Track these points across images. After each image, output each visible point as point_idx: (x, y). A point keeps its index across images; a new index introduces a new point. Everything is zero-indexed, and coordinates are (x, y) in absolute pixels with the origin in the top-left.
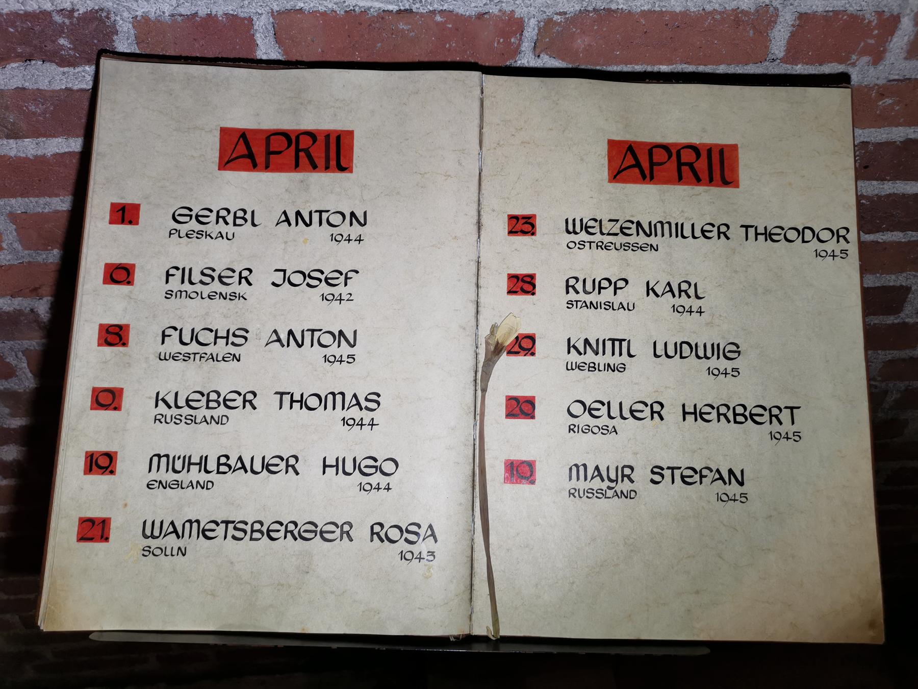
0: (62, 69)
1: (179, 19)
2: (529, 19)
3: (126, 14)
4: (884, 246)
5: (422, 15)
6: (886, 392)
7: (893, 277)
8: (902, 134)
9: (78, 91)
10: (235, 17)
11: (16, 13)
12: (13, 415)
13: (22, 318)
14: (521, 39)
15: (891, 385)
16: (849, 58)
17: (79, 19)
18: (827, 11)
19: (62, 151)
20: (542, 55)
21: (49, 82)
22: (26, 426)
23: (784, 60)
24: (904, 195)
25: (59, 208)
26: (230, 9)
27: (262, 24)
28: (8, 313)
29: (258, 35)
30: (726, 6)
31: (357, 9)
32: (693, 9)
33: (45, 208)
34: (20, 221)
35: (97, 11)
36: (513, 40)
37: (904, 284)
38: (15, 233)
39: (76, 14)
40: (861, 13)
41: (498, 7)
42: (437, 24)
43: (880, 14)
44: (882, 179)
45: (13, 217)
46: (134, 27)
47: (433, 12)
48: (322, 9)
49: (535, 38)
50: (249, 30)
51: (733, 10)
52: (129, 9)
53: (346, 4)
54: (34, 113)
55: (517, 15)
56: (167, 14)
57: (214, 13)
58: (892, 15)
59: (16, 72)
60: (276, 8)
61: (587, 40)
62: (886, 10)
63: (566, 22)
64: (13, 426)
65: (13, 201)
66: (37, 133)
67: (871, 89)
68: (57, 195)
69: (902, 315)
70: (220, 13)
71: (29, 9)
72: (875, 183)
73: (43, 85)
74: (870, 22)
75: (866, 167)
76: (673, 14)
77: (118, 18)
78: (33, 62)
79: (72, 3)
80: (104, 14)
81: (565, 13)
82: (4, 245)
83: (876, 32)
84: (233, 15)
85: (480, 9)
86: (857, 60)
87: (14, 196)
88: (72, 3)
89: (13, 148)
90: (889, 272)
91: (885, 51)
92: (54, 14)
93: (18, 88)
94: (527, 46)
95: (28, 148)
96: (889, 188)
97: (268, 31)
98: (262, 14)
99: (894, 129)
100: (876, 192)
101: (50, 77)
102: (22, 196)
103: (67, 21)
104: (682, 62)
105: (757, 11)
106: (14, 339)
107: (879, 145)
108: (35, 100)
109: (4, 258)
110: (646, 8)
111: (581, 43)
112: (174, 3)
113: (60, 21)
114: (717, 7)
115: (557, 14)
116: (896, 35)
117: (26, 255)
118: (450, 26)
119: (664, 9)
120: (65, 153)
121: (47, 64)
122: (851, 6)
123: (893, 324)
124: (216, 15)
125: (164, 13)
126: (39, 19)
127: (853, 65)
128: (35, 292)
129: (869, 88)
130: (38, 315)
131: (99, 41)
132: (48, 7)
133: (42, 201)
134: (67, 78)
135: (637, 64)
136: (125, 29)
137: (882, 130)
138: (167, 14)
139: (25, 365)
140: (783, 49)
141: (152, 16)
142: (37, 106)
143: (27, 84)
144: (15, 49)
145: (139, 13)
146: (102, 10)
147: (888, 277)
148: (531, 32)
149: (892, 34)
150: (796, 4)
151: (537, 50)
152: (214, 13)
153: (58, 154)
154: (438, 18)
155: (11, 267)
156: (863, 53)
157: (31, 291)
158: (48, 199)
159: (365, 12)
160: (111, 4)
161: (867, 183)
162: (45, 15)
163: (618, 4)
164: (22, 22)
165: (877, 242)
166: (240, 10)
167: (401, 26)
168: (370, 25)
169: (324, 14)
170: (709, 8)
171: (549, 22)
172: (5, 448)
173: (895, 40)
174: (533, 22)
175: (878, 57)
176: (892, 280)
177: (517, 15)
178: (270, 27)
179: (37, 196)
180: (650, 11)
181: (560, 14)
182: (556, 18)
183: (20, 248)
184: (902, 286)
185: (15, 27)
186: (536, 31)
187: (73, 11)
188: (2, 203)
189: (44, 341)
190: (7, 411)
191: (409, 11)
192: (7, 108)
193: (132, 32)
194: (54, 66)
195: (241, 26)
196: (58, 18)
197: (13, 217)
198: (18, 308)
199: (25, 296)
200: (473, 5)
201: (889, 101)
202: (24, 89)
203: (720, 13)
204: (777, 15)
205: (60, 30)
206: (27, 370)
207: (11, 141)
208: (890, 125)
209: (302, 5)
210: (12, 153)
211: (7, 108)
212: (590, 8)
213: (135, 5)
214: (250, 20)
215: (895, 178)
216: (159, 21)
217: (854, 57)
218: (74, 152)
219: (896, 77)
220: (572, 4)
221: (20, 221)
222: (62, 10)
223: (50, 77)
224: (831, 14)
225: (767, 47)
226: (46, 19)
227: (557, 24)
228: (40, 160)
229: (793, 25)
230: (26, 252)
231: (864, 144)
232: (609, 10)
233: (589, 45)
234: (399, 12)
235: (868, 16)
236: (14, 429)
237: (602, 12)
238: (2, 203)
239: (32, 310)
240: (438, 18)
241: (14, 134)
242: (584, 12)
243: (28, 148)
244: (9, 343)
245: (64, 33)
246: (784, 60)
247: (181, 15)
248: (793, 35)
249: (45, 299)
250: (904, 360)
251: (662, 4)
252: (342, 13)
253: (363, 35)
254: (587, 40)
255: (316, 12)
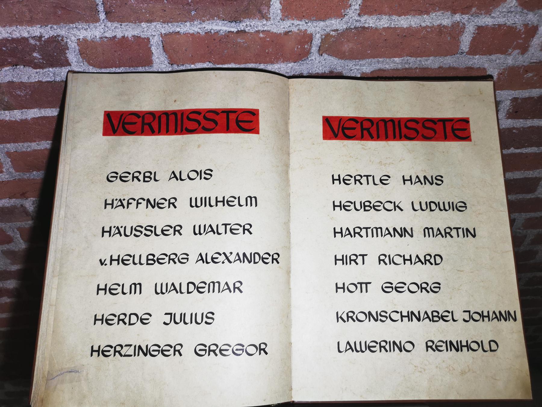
0: (35, 70)
1: (105, 40)
2: (316, 34)
3: (73, 38)
4: (527, 155)
5: (251, 34)
6: (525, 236)
7: (531, 172)
8: (538, 93)
9: (46, 82)
10: (139, 37)
11: (7, 39)
12: (13, 264)
13: (16, 210)
14: (311, 45)
15: (529, 232)
16: (507, 51)
17: (45, 41)
18: (494, 25)
19: (37, 116)
20: (323, 55)
21: (28, 78)
22: (20, 270)
23: (468, 53)
24: (538, 127)
25: (36, 148)
26: (136, 33)
27: (155, 41)
28: (7, 208)
29: (153, 47)
30: (434, 23)
31: (212, 31)
32: (414, 26)
33: (27, 149)
34: (14, 157)
35: (56, 37)
36: (306, 46)
37: (538, 176)
38: (10, 163)
39: (43, 39)
40: (515, 25)
41: (297, 28)
42: (261, 38)
43: (526, 25)
44: (525, 118)
45: (8, 154)
46: (78, 45)
47: (258, 32)
48: (191, 32)
49: (319, 44)
50: (148, 45)
51: (439, 26)
52: (75, 35)
53: (206, 28)
54: (20, 96)
55: (308, 32)
56: (98, 37)
57: (126, 36)
58: (533, 26)
59: (8, 73)
60: (163, 32)
61: (351, 45)
62: (530, 23)
63: (338, 35)
64: (13, 270)
65: (8, 145)
66: (21, 106)
67: (521, 67)
68: (35, 141)
69: (536, 193)
70: (130, 36)
71: (14, 37)
72: (521, 120)
73: (25, 79)
74: (520, 30)
75: (516, 112)
76: (402, 29)
77: (68, 40)
78: (18, 67)
79: (40, 33)
80: (60, 39)
81: (337, 30)
82: (4, 170)
83: (524, 36)
84: (137, 36)
85: (286, 29)
86: (512, 52)
87: (9, 143)
88: (40, 33)
89: (7, 116)
90: (529, 169)
91: (529, 46)
92: (30, 39)
93: (9, 81)
94: (314, 49)
95: (17, 115)
96: (529, 123)
97: (159, 45)
98: (154, 36)
99: (534, 90)
100: (522, 125)
101: (28, 75)
102: (14, 142)
103: (38, 43)
104: (407, 56)
105: (452, 26)
106: (11, 222)
107: (525, 100)
108: (20, 88)
109: (4, 177)
110: (386, 26)
111: (346, 47)
112: (102, 31)
113: (34, 43)
114: (428, 24)
115: (333, 31)
116: (535, 37)
117: (17, 175)
118: (268, 39)
119: (397, 26)
120: (39, 117)
121: (27, 68)
122: (509, 21)
123: (531, 198)
124: (127, 37)
125: (96, 36)
126: (21, 42)
127: (510, 54)
128: (24, 195)
129: (519, 67)
130: (26, 208)
131: (57, 54)
132: (26, 35)
133: (26, 145)
134: (39, 75)
135: (381, 58)
136: (73, 46)
137: (526, 91)
138: (98, 37)
139: (19, 236)
140: (468, 47)
141: (89, 38)
142: (21, 92)
143: (15, 79)
144: (7, 60)
145: (81, 37)
146: (59, 36)
147: (528, 172)
148: (317, 41)
149: (533, 36)
150: (476, 21)
151: (321, 51)
152: (126, 36)
153: (34, 118)
154: (261, 35)
155: (8, 182)
156: (514, 49)
157: (21, 195)
158: (29, 144)
159: (217, 33)
160: (64, 32)
161: (517, 120)
162: (25, 39)
163: (369, 24)
164: (10, 44)
165: (522, 153)
166: (142, 34)
167: (239, 40)
168: (220, 40)
169: (193, 35)
170: (423, 25)
171: (328, 35)
172: (9, 282)
173: (535, 40)
174: (318, 36)
175: (524, 49)
176: (530, 174)
177: (308, 32)
178: (160, 43)
179: (23, 142)
180: (388, 28)
181: (334, 31)
182: (332, 33)
183: (13, 171)
184: (536, 178)
185: (7, 47)
186: (320, 41)
187: (41, 37)
188: (2, 147)
189: (30, 222)
190: (9, 261)
191: (243, 32)
192: (3, 93)
193: (77, 48)
194: (31, 69)
195: (142, 44)
196: (32, 42)
197: (8, 154)
198: (13, 204)
199: (16, 198)
200: (282, 27)
201: (530, 75)
202: (13, 82)
203: (430, 27)
204: (465, 28)
205: (34, 48)
206: (20, 239)
207: (6, 112)
208: (530, 88)
209: (179, 30)
210: (7, 119)
211: (3, 93)
212: (352, 27)
213: (78, 32)
214: (148, 39)
215: (533, 118)
216: (93, 41)
217: (510, 50)
218: (44, 117)
219: (535, 61)
220: (342, 25)
221: (14, 157)
222: (34, 37)
223: (28, 75)
224: (497, 26)
225: (458, 46)
226: (25, 42)
227: (332, 36)
228: (24, 122)
229: (474, 33)
230: (17, 173)
231: (515, 100)
232: (364, 28)
233: (351, 48)
234: (238, 32)
235: (519, 27)
236: (14, 271)
237: (360, 29)
238: (2, 147)
239: (22, 206)
240: (261, 35)
241: (8, 108)
242: (348, 29)
243: (17, 115)
244: (9, 224)
245: (36, 50)
246: (468, 53)
247: (106, 38)
248: (474, 39)
249: (29, 199)
250: (537, 218)
251: (395, 23)
252: (203, 34)
253: (216, 46)
254: (351, 45)
255: (188, 33)
